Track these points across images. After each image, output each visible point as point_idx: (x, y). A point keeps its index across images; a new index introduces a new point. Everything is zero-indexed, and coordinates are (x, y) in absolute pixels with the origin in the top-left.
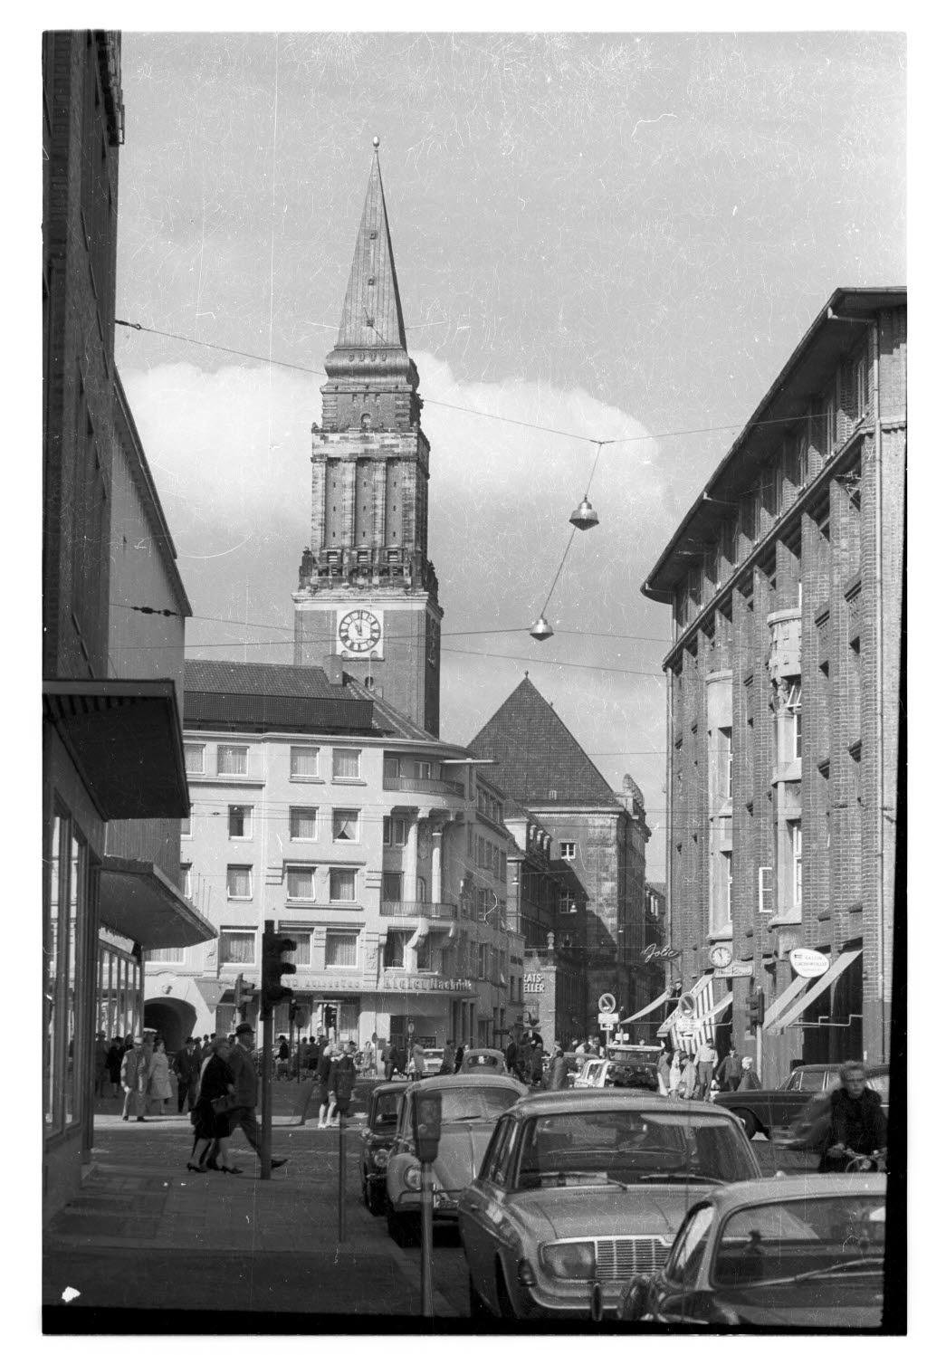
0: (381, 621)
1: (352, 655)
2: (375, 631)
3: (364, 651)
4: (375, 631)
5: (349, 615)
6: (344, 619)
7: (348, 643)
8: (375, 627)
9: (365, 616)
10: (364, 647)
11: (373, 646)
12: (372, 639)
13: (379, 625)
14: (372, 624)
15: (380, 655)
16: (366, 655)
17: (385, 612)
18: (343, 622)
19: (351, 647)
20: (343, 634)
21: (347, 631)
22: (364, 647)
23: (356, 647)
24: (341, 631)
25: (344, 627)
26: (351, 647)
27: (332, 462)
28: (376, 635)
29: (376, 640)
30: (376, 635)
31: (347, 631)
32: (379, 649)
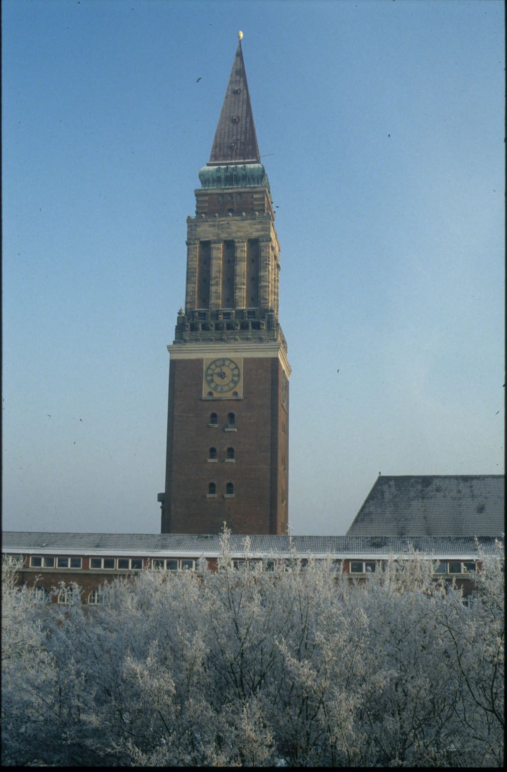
0: (242, 371)
1: (216, 395)
3: (227, 392)
6: (210, 365)
7: (213, 385)
8: (236, 372)
9: (227, 363)
10: (226, 388)
11: (233, 388)
13: (239, 370)
14: (233, 370)
16: (229, 395)
18: (209, 368)
20: (209, 378)
22: (226, 388)
23: (219, 389)
24: (206, 376)
29: (236, 383)
30: (236, 379)
32: (240, 389)
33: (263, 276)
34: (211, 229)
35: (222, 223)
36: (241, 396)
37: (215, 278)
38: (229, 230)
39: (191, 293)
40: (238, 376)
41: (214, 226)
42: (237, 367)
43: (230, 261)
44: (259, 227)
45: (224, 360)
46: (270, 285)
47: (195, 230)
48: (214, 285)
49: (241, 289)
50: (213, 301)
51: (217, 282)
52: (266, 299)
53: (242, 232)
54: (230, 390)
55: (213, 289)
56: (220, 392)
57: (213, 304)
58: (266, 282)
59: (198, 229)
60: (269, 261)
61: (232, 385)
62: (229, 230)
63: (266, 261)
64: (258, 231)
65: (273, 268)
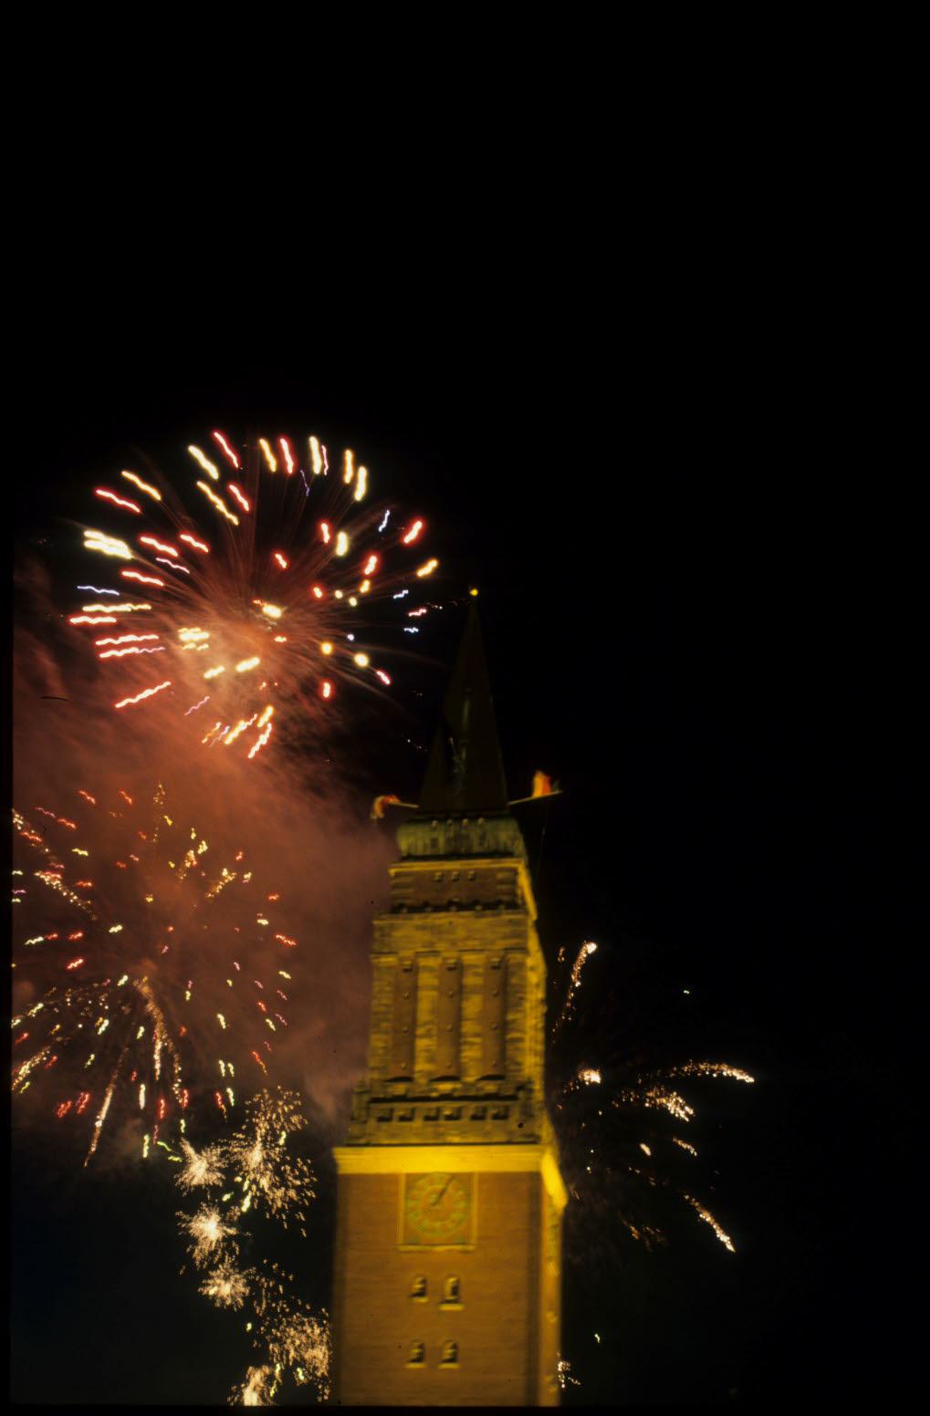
33: (514, 1021)
34: (419, 935)
35: (438, 922)
37: (426, 1023)
38: (452, 937)
39: (381, 1052)
41: (423, 928)
43: (457, 993)
44: (507, 930)
46: (527, 1037)
47: (389, 935)
48: (422, 1037)
49: (472, 1044)
50: (421, 1066)
51: (429, 1030)
52: (518, 1064)
53: (476, 939)
55: (421, 1043)
57: (420, 1072)
58: (518, 1031)
59: (397, 934)
60: (525, 993)
62: (452, 937)
63: (518, 992)
64: (505, 937)
65: (534, 1004)
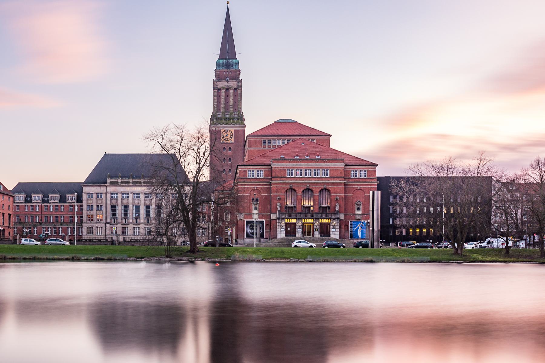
1: (225, 142)
2: (231, 135)
3: (229, 140)
4: (231, 135)
5: (224, 131)
7: (224, 138)
8: (231, 134)
9: (229, 131)
12: (231, 137)
15: (233, 142)
17: (234, 130)
18: (223, 133)
19: (225, 140)
20: (223, 136)
21: (224, 135)
22: (228, 139)
23: (226, 140)
24: (222, 135)
25: (223, 134)
26: (225, 140)
27: (220, 89)
28: (231, 136)
30: (231, 136)
31: (224, 135)
32: (232, 140)
36: (233, 142)
40: (232, 135)
42: (232, 133)
45: (228, 130)
54: (230, 140)
56: (227, 141)
61: (230, 138)
